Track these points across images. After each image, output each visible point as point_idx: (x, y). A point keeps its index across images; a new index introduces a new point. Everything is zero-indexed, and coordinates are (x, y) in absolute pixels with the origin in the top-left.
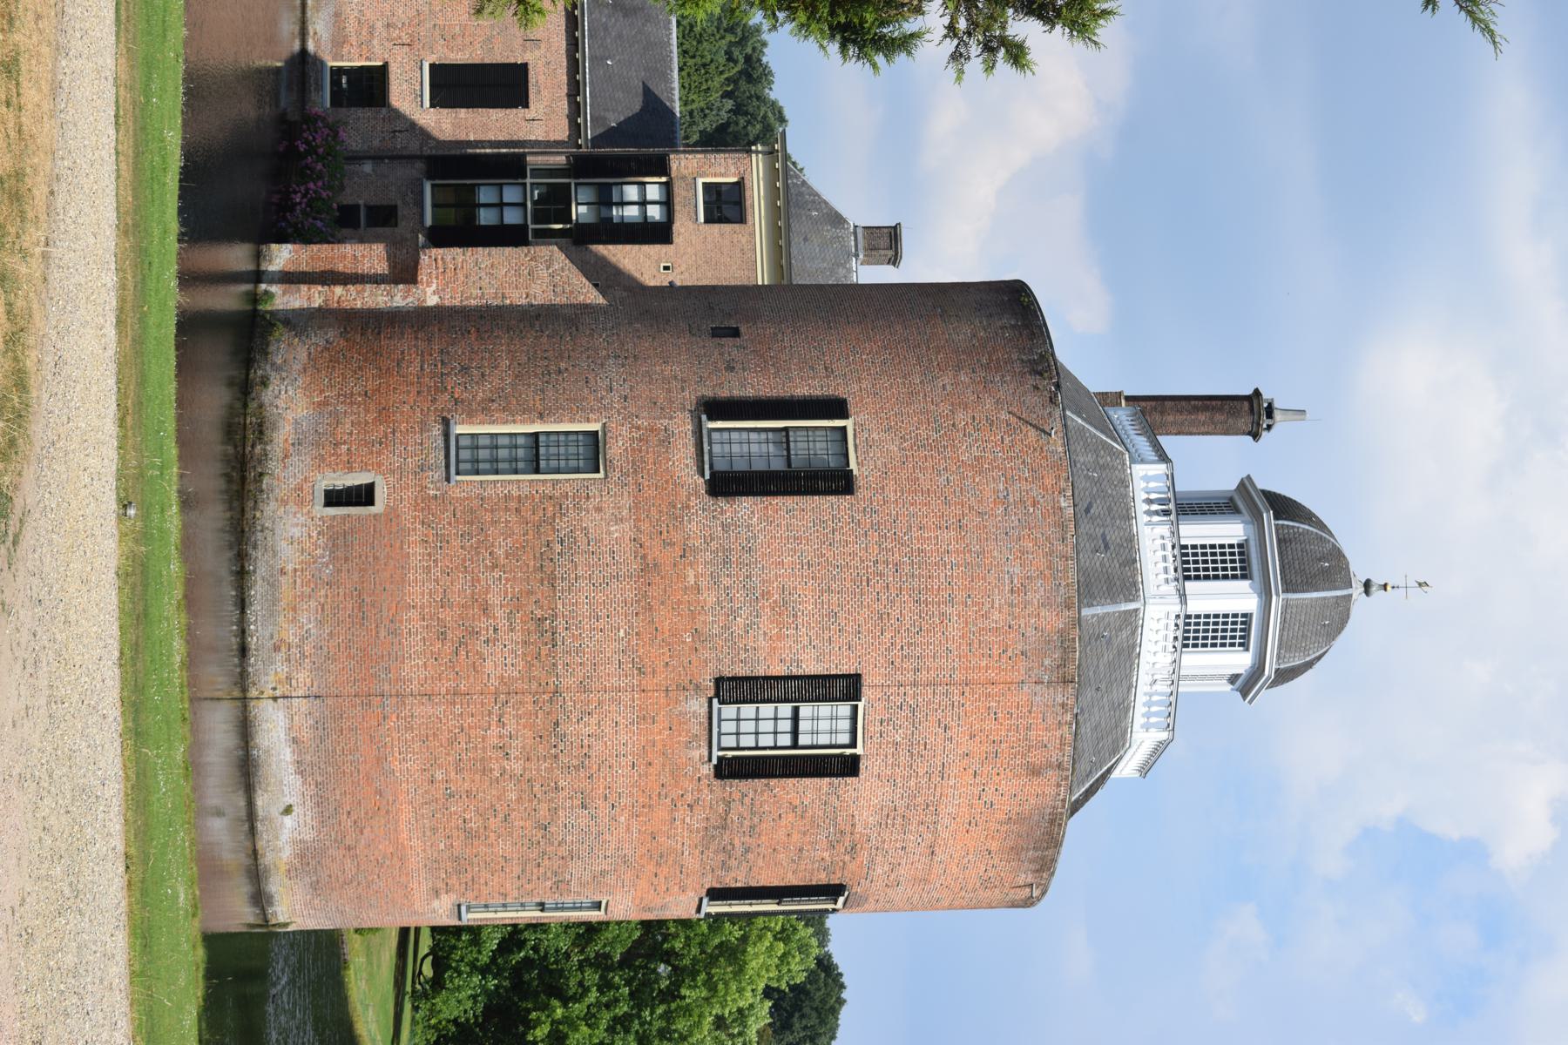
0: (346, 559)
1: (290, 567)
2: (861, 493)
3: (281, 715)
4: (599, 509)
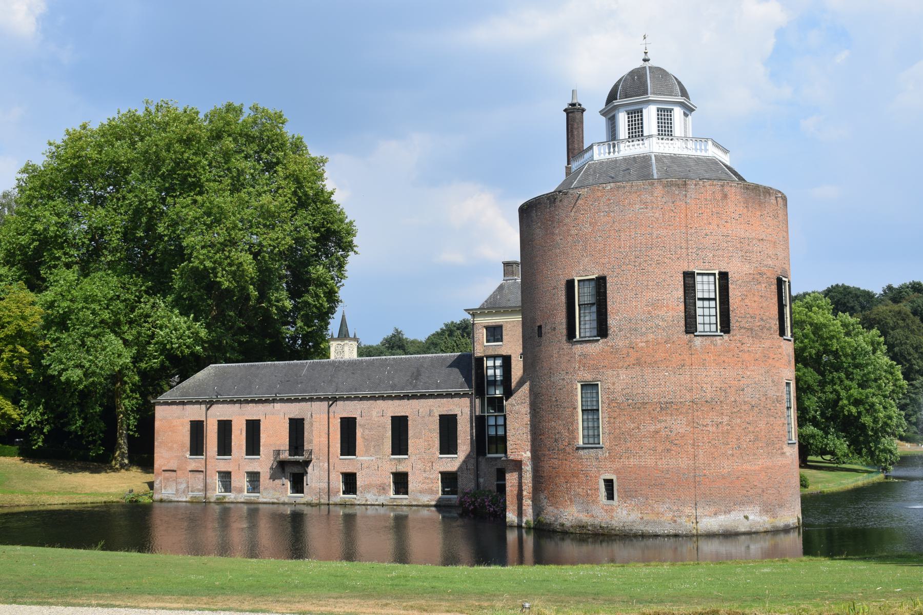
0: (636, 491)
1: (640, 515)
2: (606, 273)
4: (614, 384)
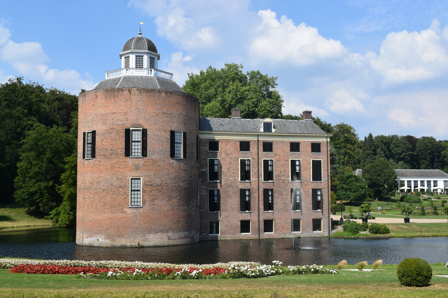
3: (85, 239)
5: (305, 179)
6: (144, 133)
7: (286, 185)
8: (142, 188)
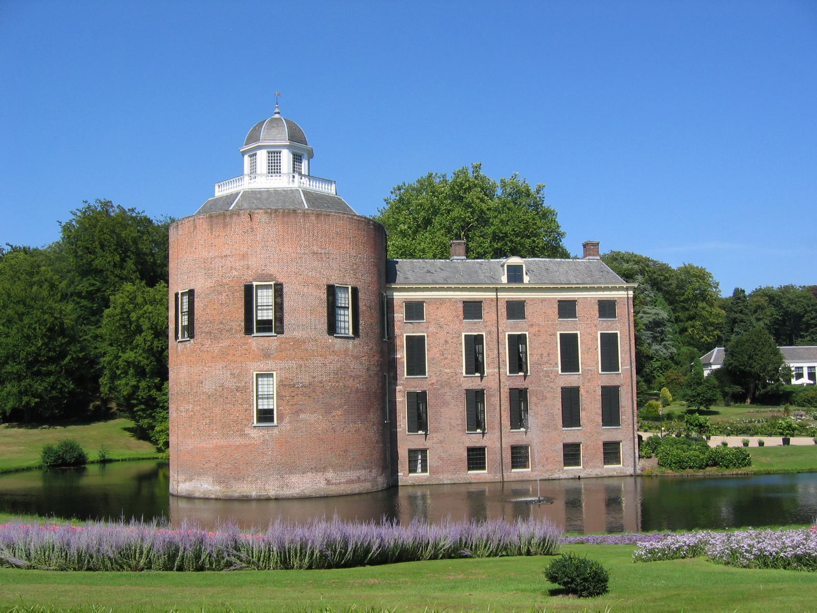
5: (588, 368)
6: (279, 291)
7: (552, 380)
8: (277, 391)
